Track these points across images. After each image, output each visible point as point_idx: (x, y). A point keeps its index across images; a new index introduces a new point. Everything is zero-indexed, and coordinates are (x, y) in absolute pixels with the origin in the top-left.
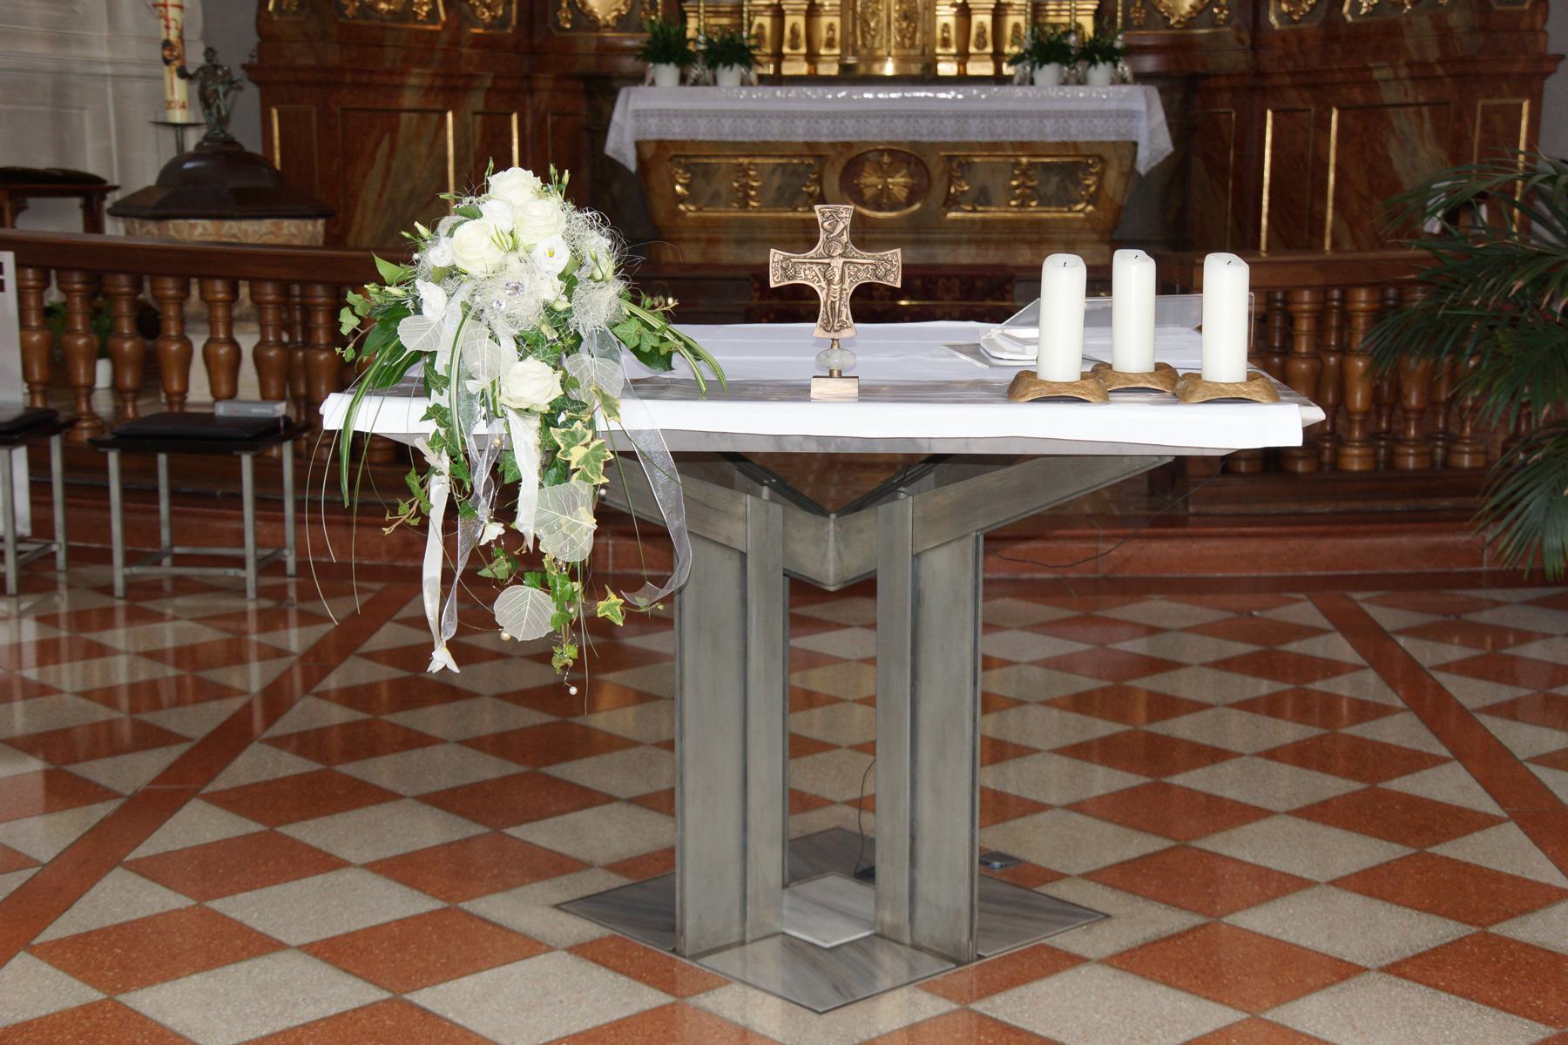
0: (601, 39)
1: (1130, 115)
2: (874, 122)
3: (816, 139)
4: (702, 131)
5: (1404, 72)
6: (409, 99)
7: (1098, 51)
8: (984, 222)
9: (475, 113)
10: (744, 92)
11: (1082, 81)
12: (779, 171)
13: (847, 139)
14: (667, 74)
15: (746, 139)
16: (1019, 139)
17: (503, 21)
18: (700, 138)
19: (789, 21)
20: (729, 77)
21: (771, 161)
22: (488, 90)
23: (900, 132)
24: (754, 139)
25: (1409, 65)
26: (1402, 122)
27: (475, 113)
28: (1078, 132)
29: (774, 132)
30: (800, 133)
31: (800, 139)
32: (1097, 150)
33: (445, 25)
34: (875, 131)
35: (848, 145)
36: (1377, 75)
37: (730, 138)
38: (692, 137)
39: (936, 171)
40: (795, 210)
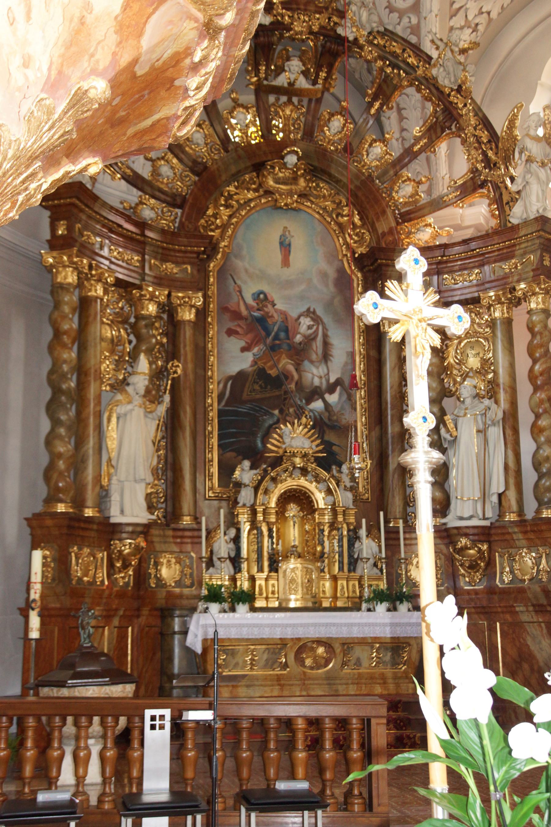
0: (168, 592)
2: (312, 629)
3: (285, 637)
5: (531, 608)
8: (359, 674)
9: (115, 627)
10: (222, 615)
12: (267, 652)
13: (300, 636)
14: (214, 607)
15: (254, 637)
16: (375, 636)
17: (127, 584)
18: (233, 637)
19: (258, 583)
20: (242, 609)
21: (264, 647)
22: (121, 616)
23: (322, 633)
24: (257, 637)
25: (533, 605)
26: (533, 630)
27: (115, 627)
29: (266, 634)
30: (278, 634)
31: (279, 637)
32: (407, 640)
33: (107, 586)
34: (312, 632)
35: (299, 639)
36: (517, 609)
37: (246, 637)
38: (229, 637)
39: (338, 649)
40: (274, 670)
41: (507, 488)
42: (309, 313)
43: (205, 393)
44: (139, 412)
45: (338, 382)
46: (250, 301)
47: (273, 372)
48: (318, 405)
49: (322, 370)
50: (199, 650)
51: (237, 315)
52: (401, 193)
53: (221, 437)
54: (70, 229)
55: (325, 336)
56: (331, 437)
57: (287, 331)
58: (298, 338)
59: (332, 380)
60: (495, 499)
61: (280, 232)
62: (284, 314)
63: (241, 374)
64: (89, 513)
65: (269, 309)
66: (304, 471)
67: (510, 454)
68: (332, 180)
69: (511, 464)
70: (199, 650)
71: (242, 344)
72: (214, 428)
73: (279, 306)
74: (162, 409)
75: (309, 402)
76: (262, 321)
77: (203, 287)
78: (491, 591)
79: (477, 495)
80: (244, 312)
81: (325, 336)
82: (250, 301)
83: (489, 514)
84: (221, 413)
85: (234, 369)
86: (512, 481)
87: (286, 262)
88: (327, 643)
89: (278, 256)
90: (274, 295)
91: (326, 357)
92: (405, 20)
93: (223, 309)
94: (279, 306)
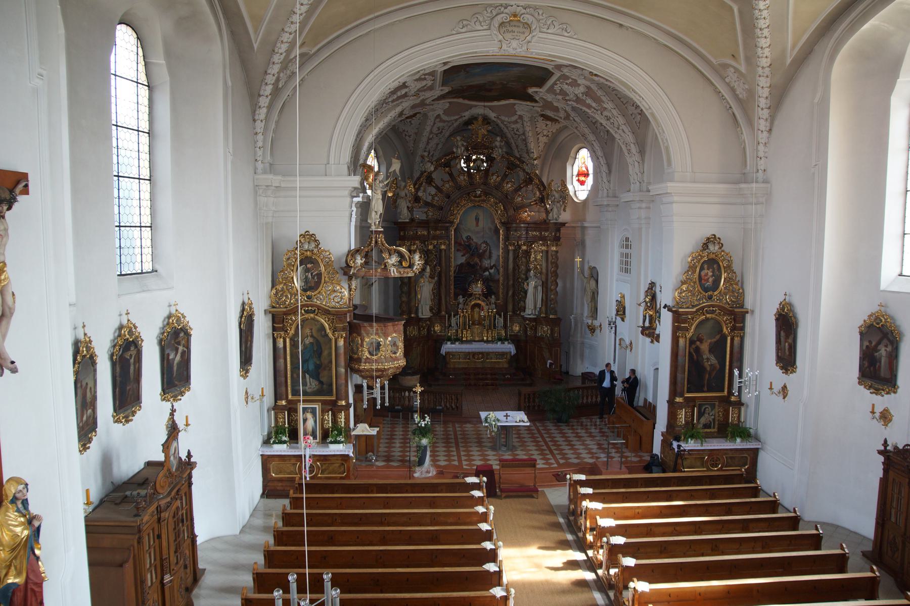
1: (510, 348)
4: (454, 351)
6: (414, 346)
7: (506, 339)
11: (504, 343)
14: (449, 343)
20: (457, 343)
28: (504, 350)
29: (463, 351)
30: (467, 351)
41: (542, 305)
42: (485, 242)
43: (450, 271)
44: (427, 283)
45: (494, 265)
46: (465, 239)
47: (472, 263)
48: (487, 273)
49: (489, 261)
50: (444, 354)
51: (460, 244)
52: (518, 200)
53: (454, 285)
54: (405, 233)
55: (490, 250)
56: (491, 284)
57: (477, 248)
58: (481, 251)
59: (492, 265)
60: (538, 309)
61: (475, 214)
62: (474, 242)
63: (462, 264)
64: (413, 315)
65: (471, 242)
66: (479, 299)
67: (544, 295)
68: (494, 197)
69: (544, 298)
70: (444, 354)
71: (462, 254)
72: (452, 282)
73: (474, 240)
74: (434, 281)
75: (484, 272)
76: (469, 246)
77: (448, 237)
78: (535, 337)
79: (533, 308)
80: (463, 243)
81: (490, 250)
82: (465, 239)
83: (537, 313)
84: (455, 277)
85: (459, 262)
86: (544, 304)
87: (477, 225)
88: (482, 353)
89: (474, 223)
90: (474, 237)
91: (490, 257)
92: (520, 137)
93: (455, 242)
94: (474, 240)
